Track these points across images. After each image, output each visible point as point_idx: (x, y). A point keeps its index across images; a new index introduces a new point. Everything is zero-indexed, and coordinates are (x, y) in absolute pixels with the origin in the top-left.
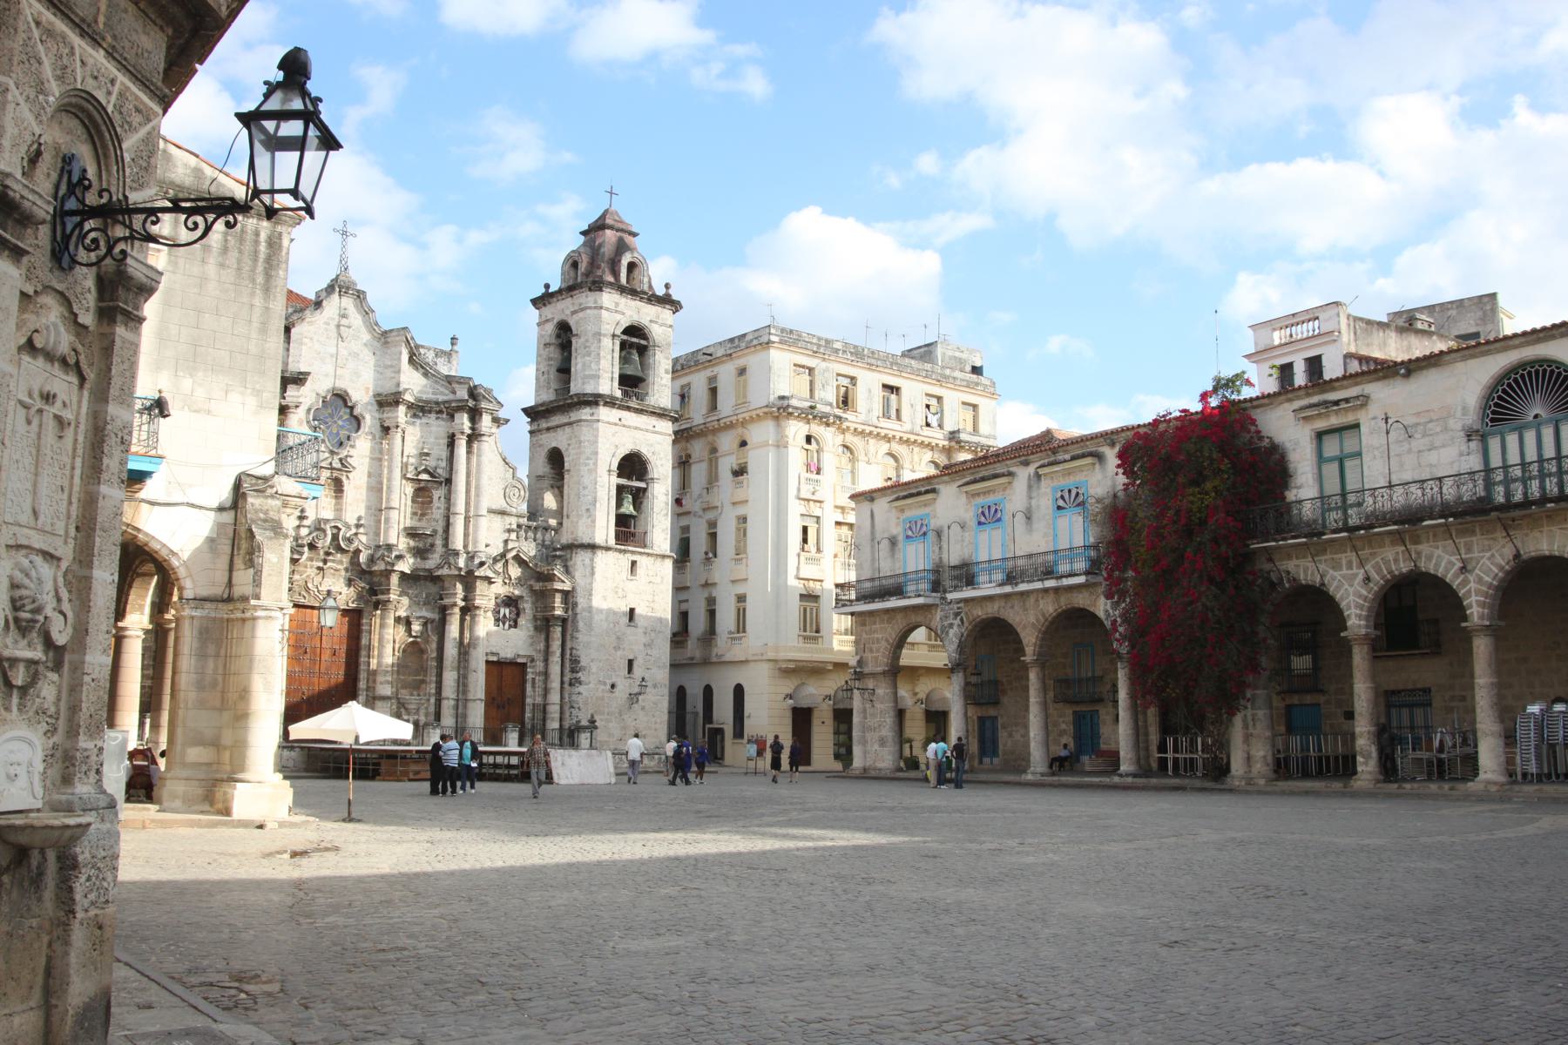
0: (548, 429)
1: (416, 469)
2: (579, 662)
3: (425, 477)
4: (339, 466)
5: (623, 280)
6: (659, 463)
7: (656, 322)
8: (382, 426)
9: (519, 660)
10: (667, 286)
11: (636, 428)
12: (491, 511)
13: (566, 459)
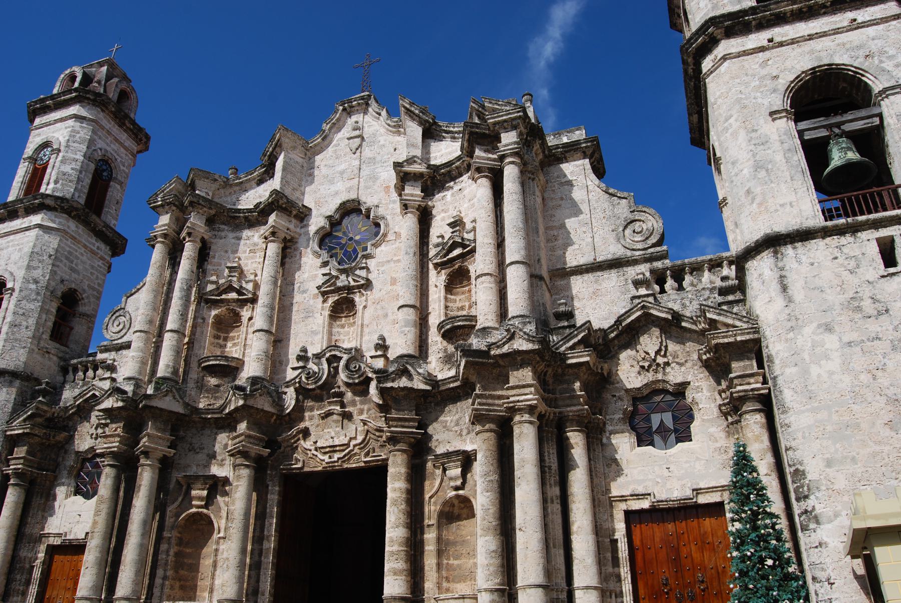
2: (803, 473)
6: (888, 65)
9: (703, 499)
11: (811, 37)
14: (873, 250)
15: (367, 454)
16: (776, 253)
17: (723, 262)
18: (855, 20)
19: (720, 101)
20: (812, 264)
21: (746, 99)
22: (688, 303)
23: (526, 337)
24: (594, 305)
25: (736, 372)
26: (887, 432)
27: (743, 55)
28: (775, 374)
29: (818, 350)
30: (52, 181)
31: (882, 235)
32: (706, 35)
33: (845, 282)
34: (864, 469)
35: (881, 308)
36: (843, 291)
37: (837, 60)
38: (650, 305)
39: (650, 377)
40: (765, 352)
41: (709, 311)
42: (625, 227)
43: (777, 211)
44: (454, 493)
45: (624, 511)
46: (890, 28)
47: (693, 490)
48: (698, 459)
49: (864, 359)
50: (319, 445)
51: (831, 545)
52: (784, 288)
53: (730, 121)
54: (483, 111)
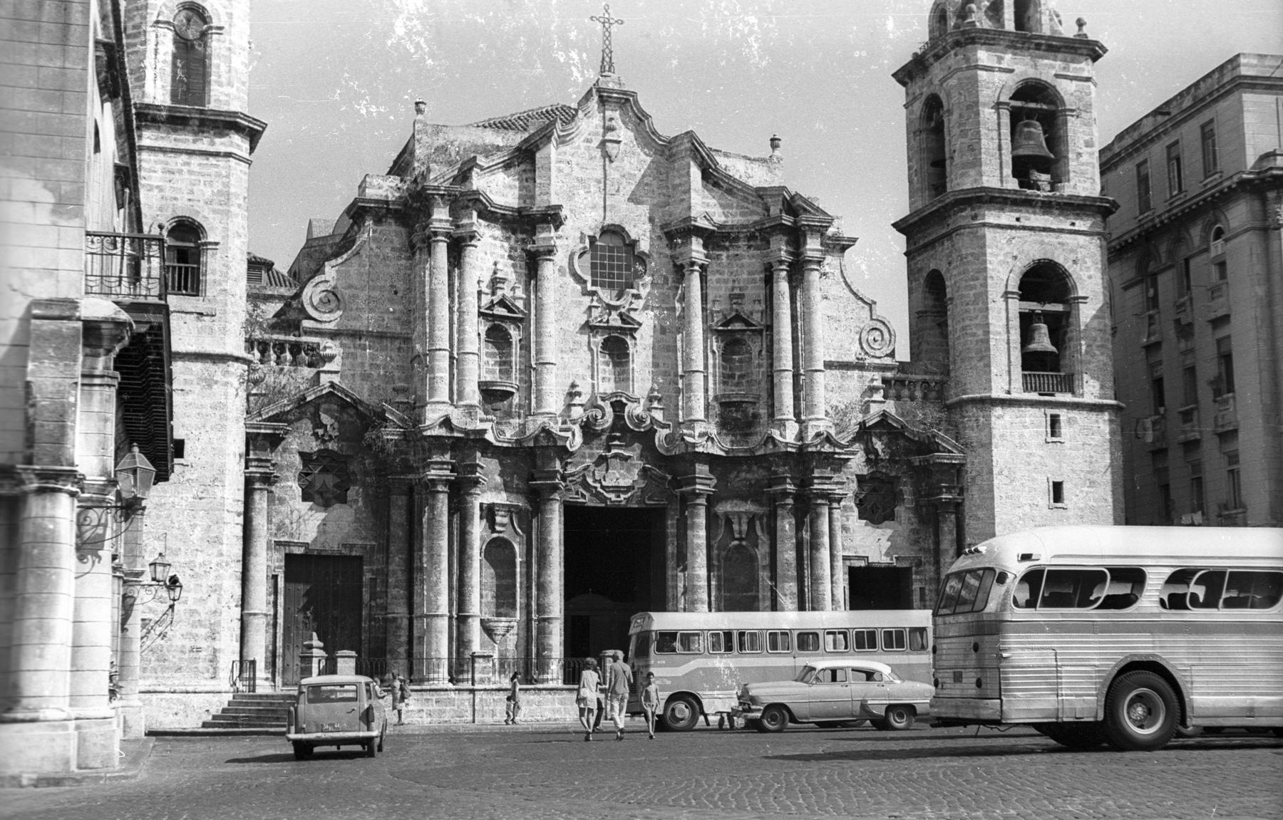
0: (926, 247)
1: (725, 317)
3: (738, 326)
4: (618, 323)
5: (1010, 25)
6: (1084, 275)
7: (1065, 77)
8: (675, 265)
10: (1080, 23)
11: (1045, 230)
12: (829, 365)
13: (948, 283)
15: (650, 499)
19: (970, 258)
30: (223, 80)
44: (736, 543)
50: (604, 483)
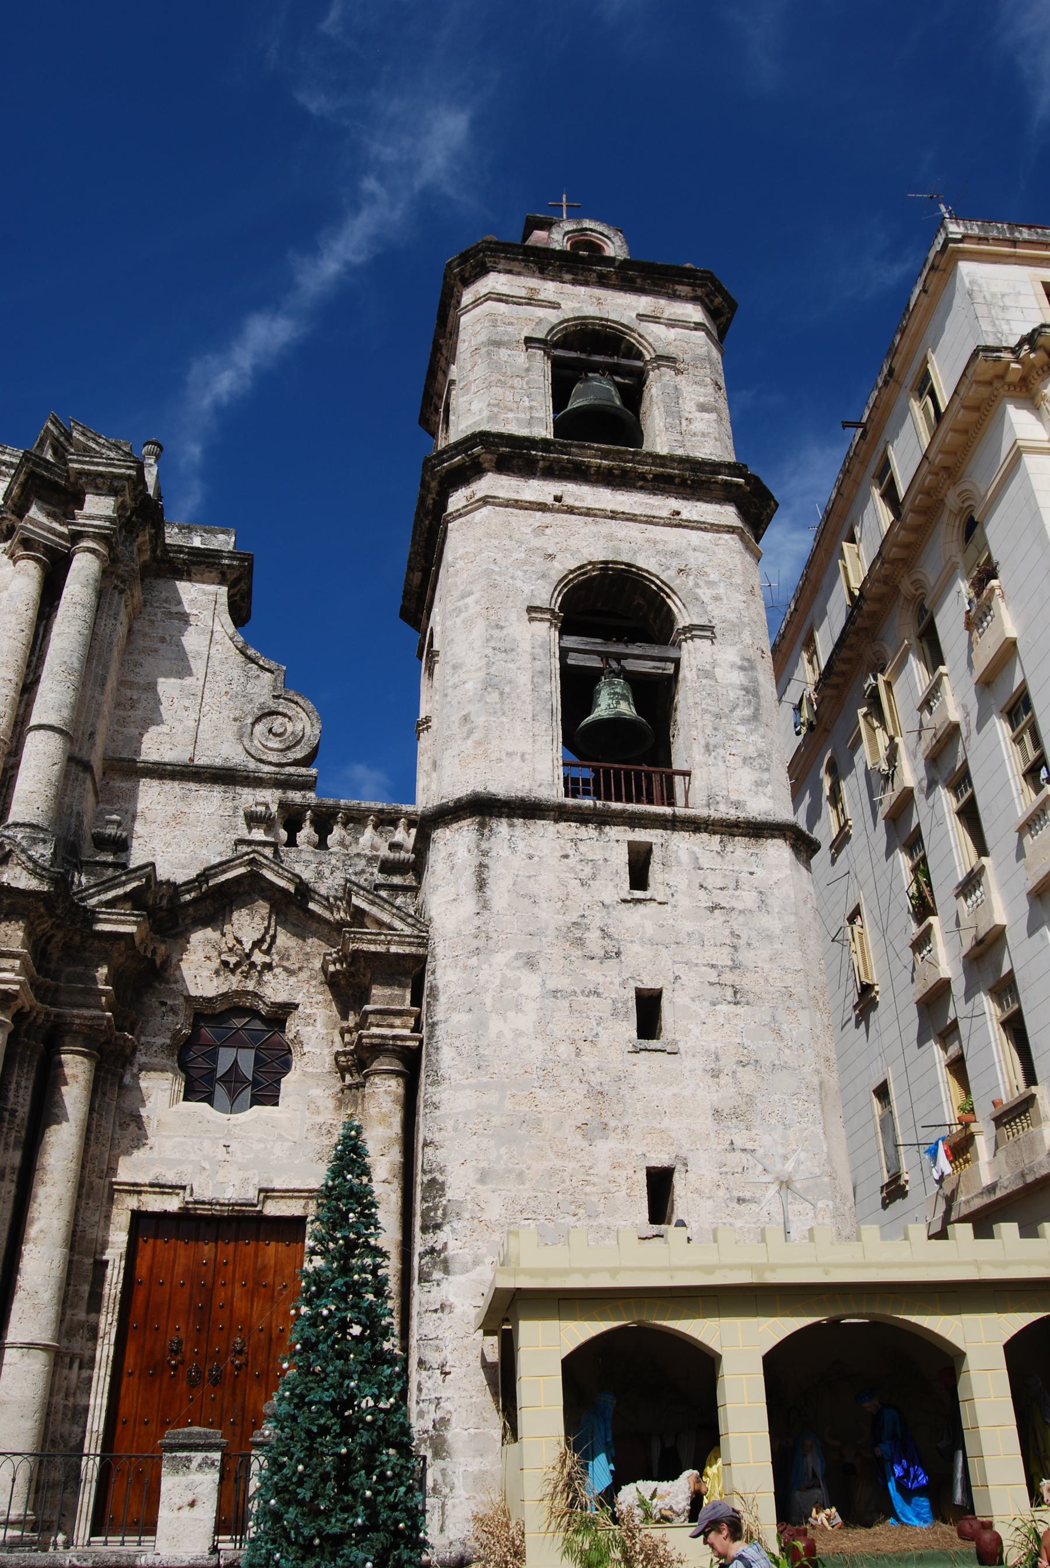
6: (705, 594)
9: (273, 1209)
11: (614, 515)
14: (621, 857)
16: (482, 825)
17: (399, 819)
18: (678, 513)
19: (460, 564)
20: (531, 857)
21: (500, 574)
22: (327, 873)
23: (30, 865)
24: (168, 837)
25: (375, 1003)
26: (577, 1140)
27: (514, 507)
28: (435, 1019)
29: (508, 993)
31: (638, 839)
32: (468, 456)
33: (571, 897)
34: (532, 1194)
35: (610, 948)
36: (565, 910)
37: (641, 562)
38: (264, 861)
39: (234, 982)
40: (428, 979)
41: (357, 894)
42: (258, 720)
43: (500, 760)
45: (133, 1211)
46: (720, 542)
47: (261, 1191)
48: (280, 1137)
49: (570, 1021)
51: (458, 1310)
52: (481, 885)
53: (470, 600)
54: (66, 444)
